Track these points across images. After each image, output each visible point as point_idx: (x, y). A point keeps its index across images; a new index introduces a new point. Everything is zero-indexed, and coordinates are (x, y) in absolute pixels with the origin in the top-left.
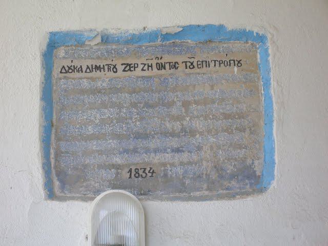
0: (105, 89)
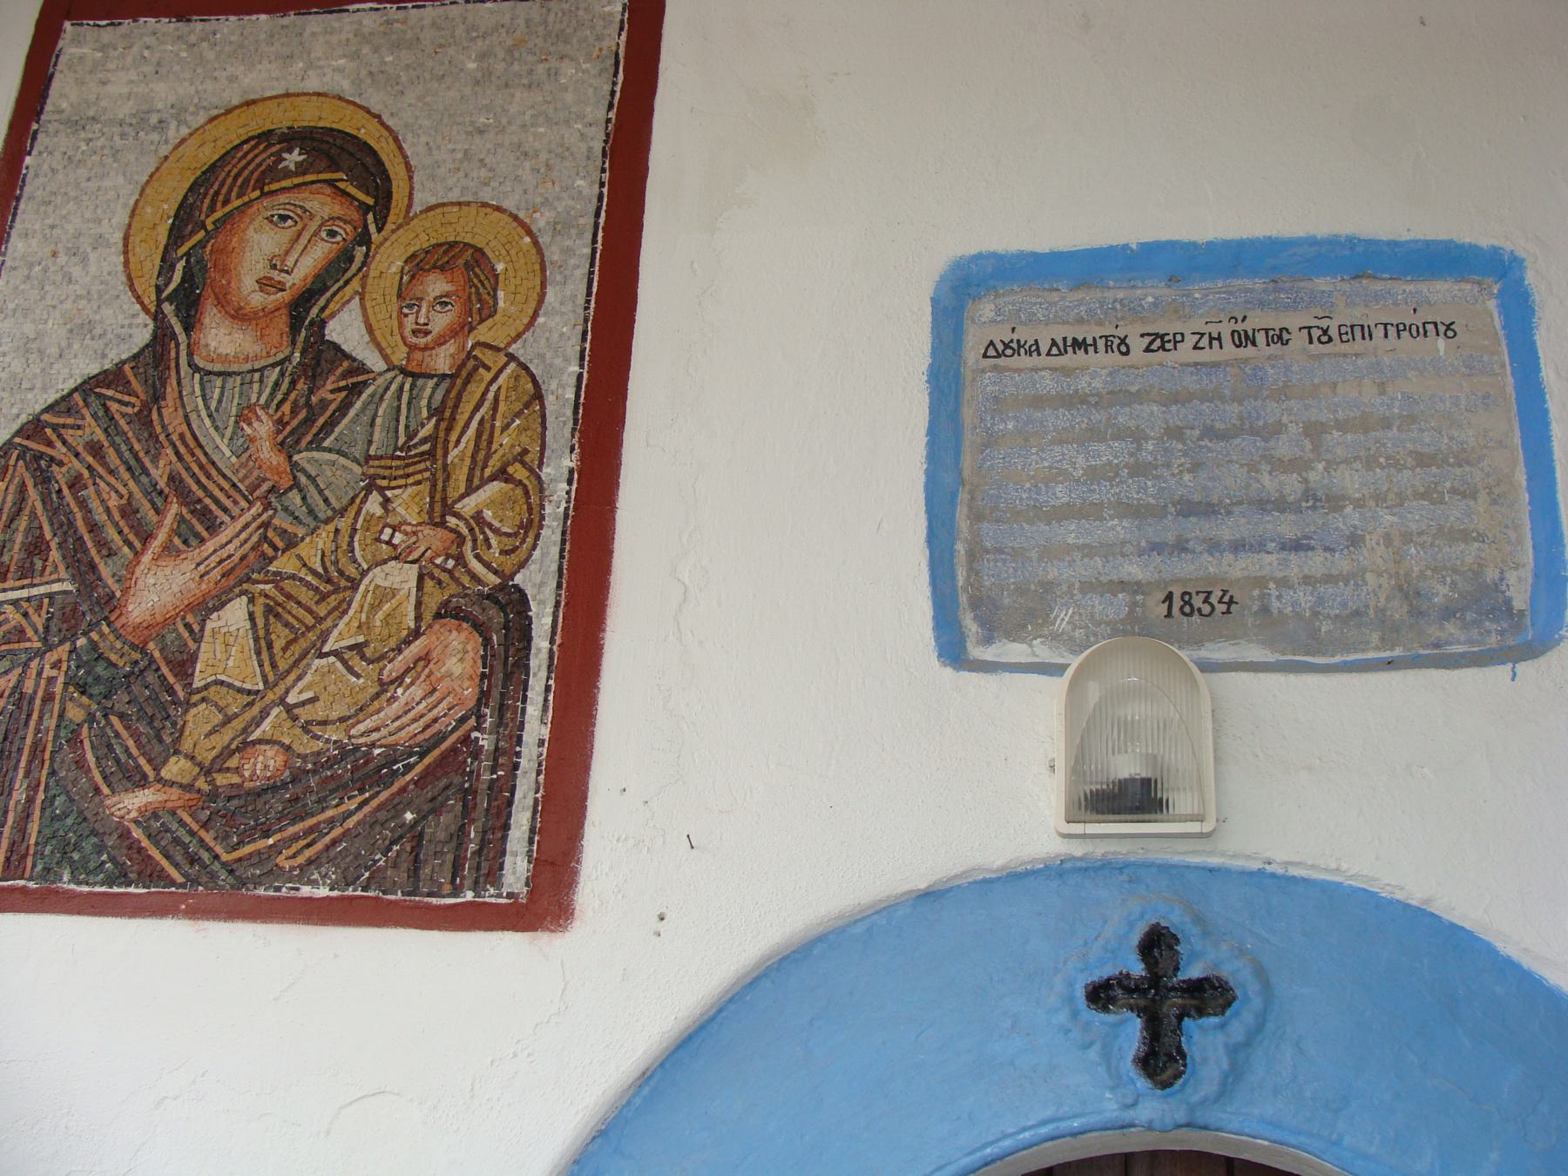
0: (1098, 395)
